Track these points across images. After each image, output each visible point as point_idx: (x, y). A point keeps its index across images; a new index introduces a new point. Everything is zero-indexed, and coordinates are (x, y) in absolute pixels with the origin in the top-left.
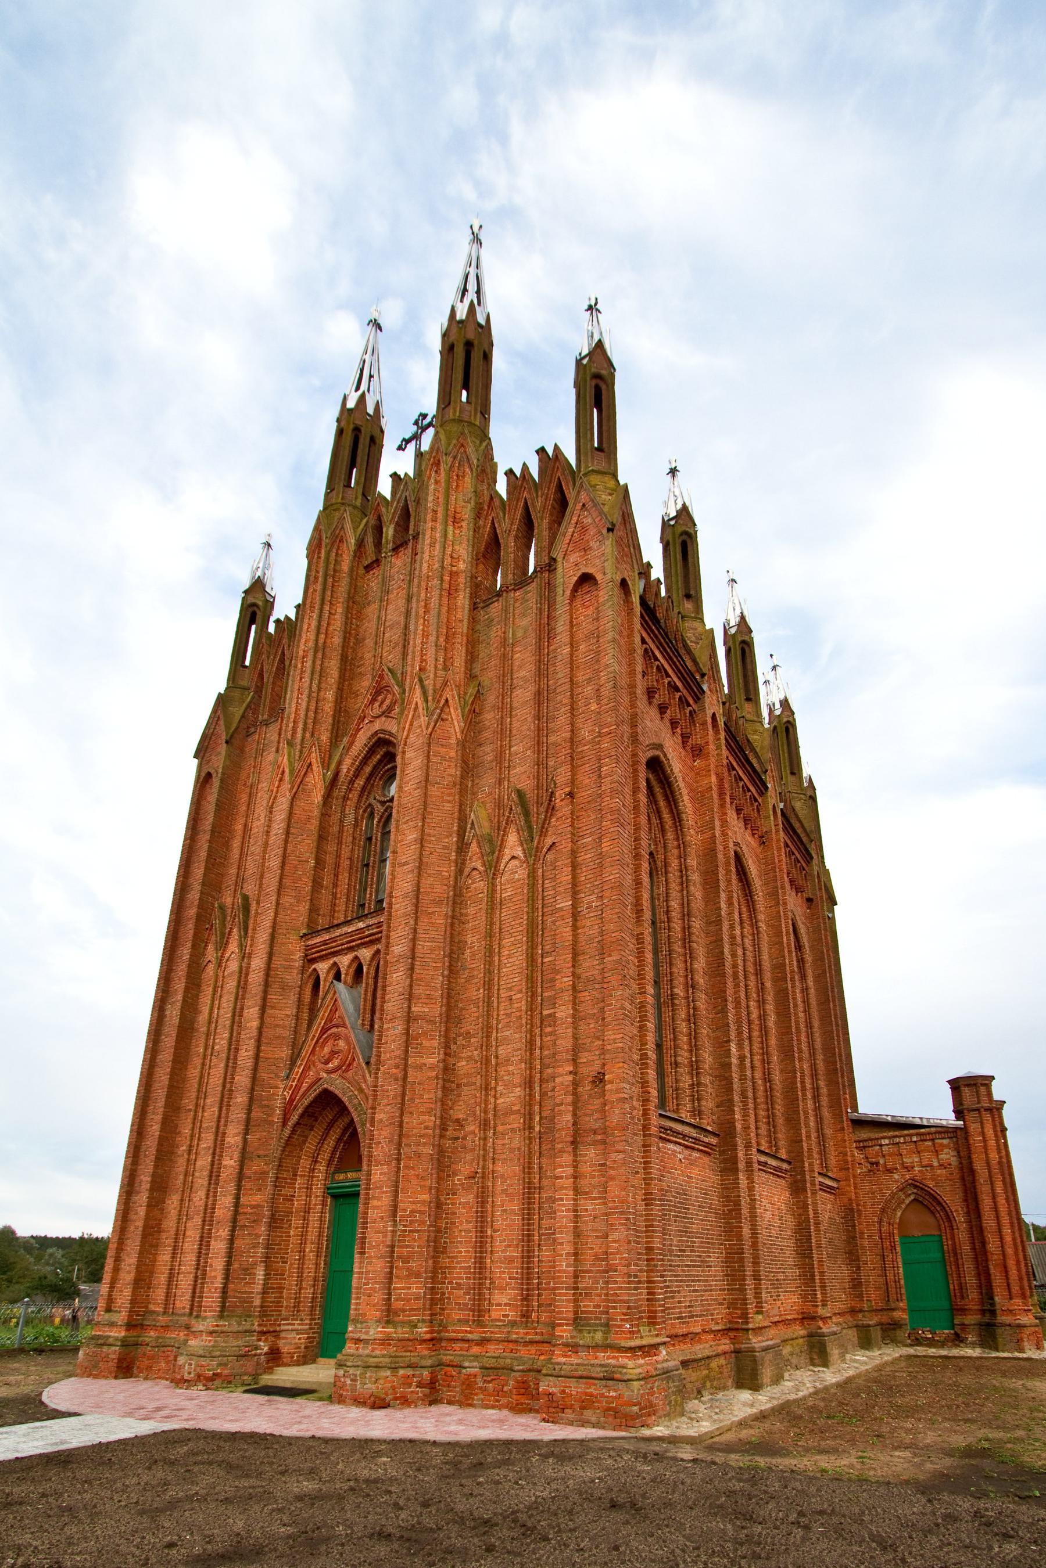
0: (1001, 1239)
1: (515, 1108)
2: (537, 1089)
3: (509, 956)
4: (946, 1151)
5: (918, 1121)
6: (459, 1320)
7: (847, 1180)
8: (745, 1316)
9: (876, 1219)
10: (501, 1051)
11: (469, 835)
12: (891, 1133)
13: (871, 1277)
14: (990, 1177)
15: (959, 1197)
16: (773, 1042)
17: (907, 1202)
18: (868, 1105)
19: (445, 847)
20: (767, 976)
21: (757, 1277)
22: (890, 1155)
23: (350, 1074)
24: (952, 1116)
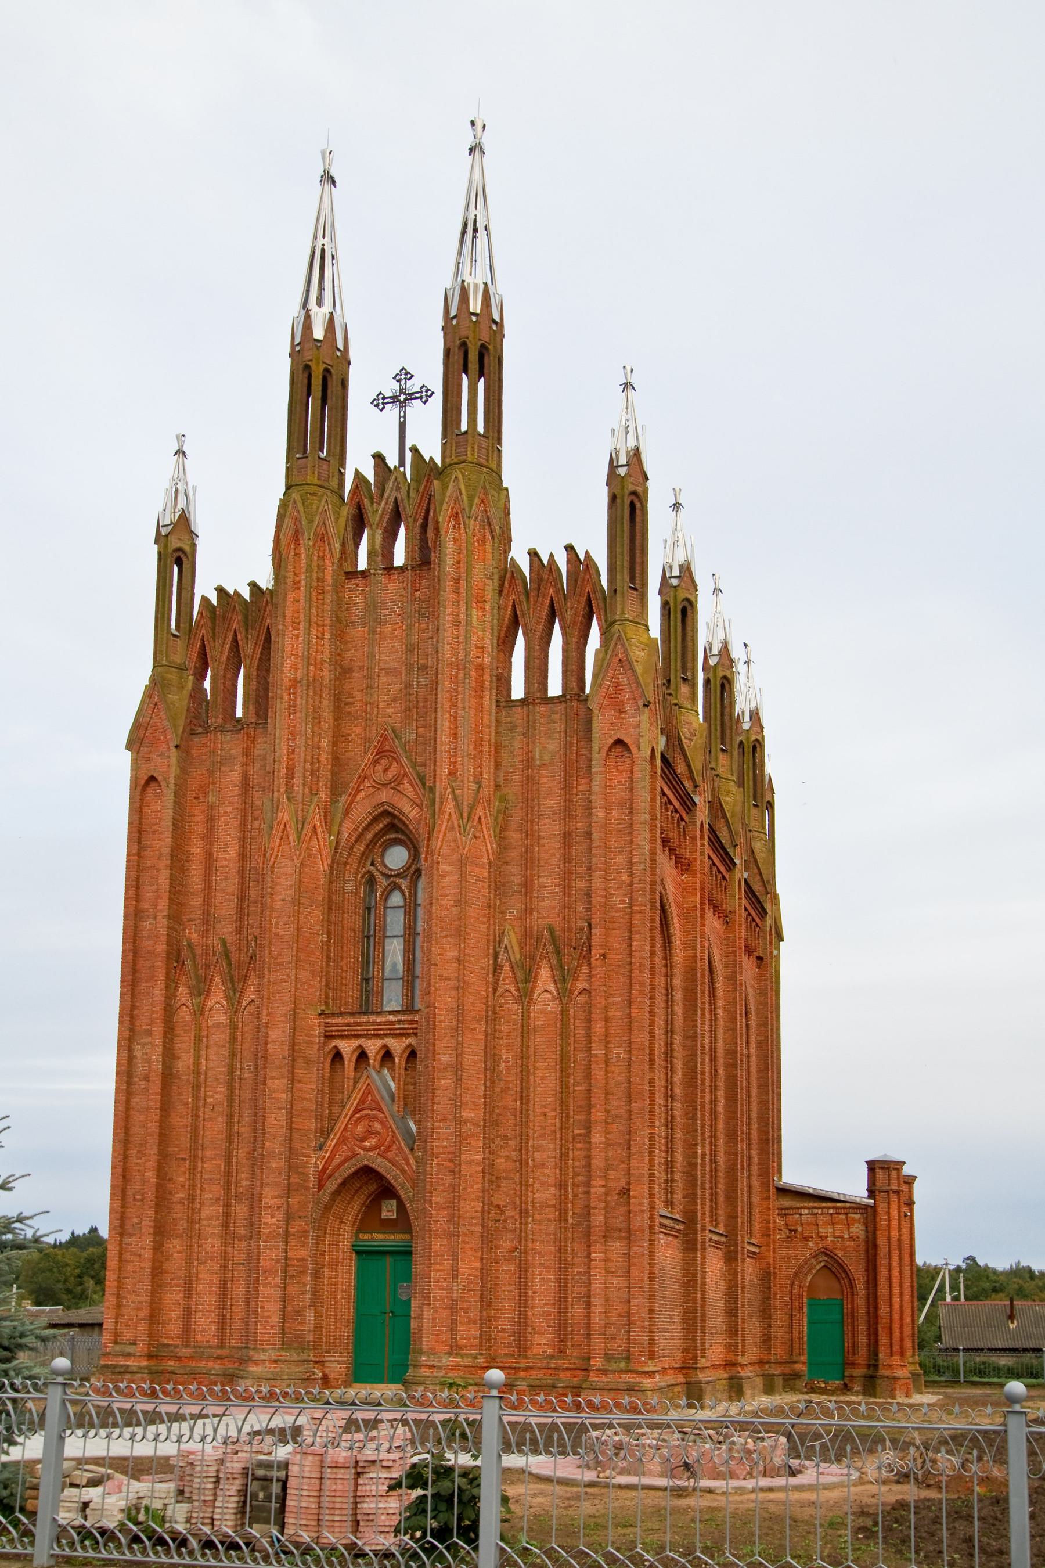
0: (891, 1305)
1: (550, 1203)
2: (570, 1190)
3: (543, 1078)
4: (856, 1225)
5: (836, 1196)
6: (505, 1355)
7: (768, 1245)
8: (695, 1359)
9: (789, 1282)
10: (538, 1156)
11: (502, 958)
12: (811, 1204)
13: (779, 1334)
14: (890, 1252)
15: (862, 1266)
16: (721, 1126)
17: (818, 1267)
18: (792, 1175)
19: (482, 968)
20: (721, 1061)
21: (703, 1332)
22: (809, 1224)
23: (390, 1155)
24: (866, 1194)
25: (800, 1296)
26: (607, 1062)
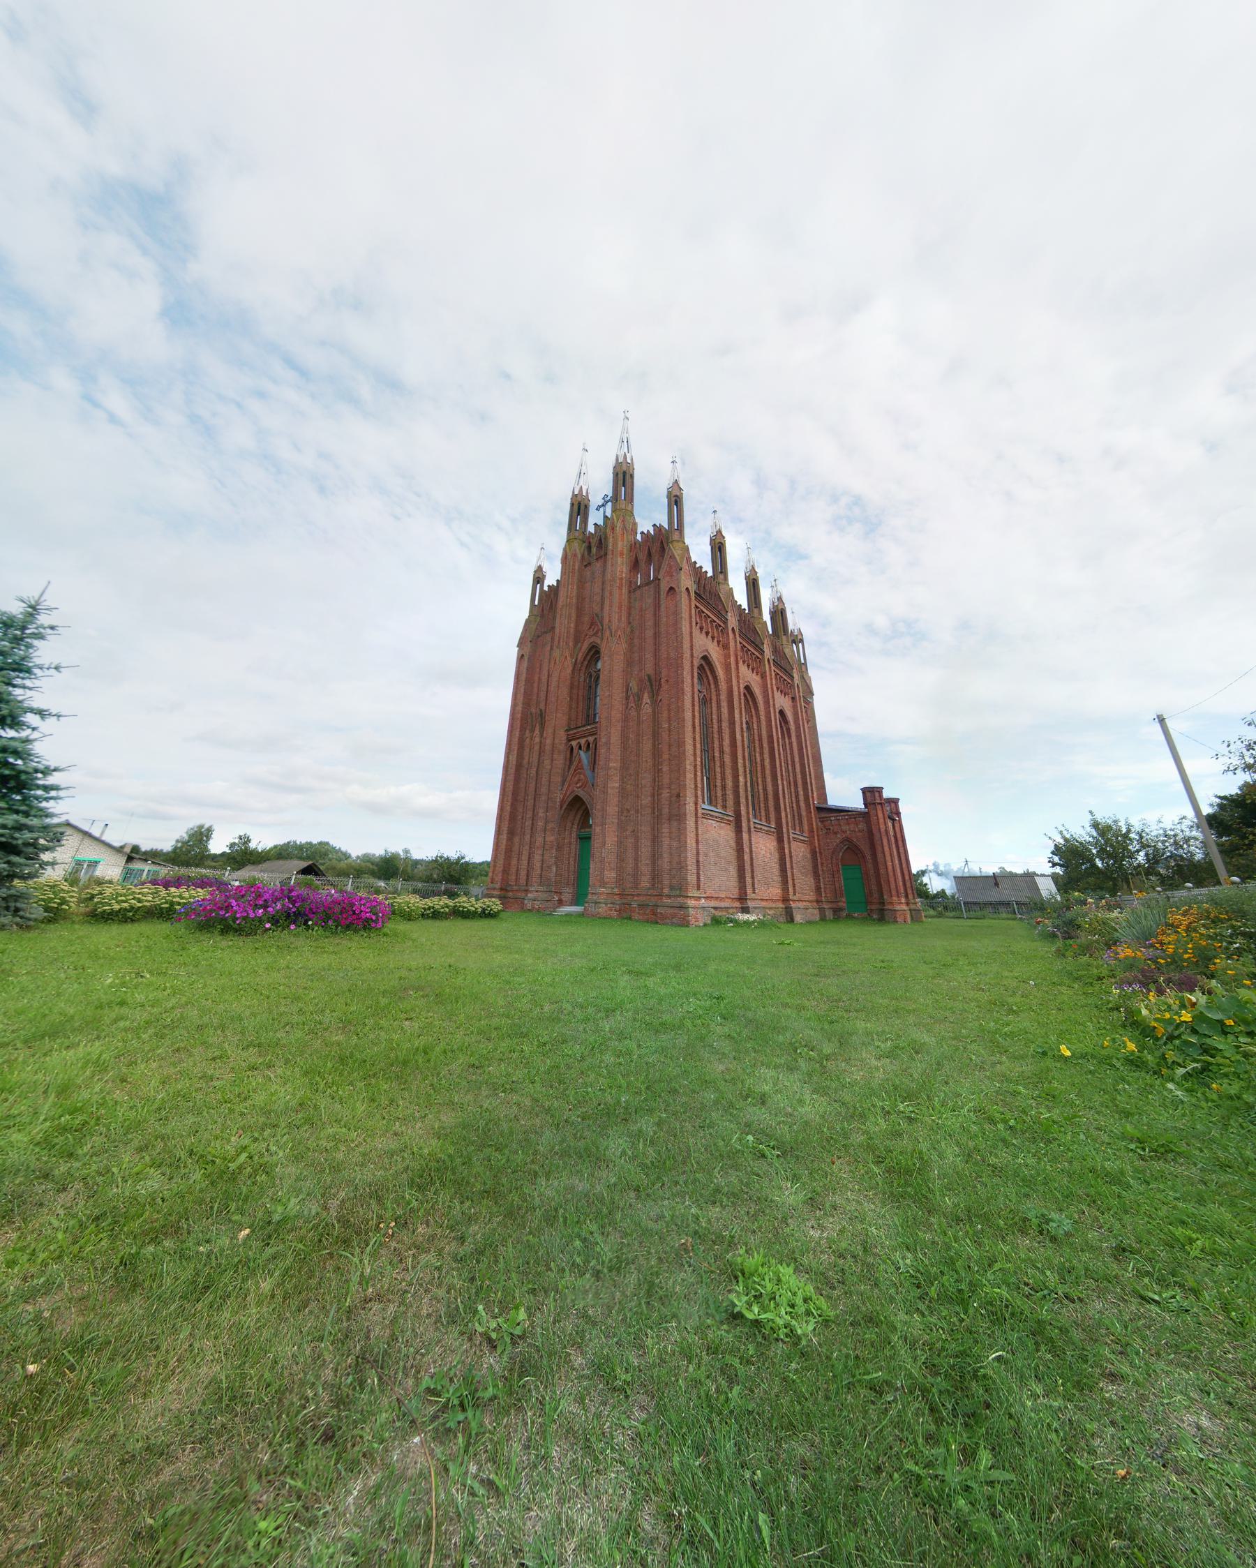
25: (837, 865)
26: (670, 730)
